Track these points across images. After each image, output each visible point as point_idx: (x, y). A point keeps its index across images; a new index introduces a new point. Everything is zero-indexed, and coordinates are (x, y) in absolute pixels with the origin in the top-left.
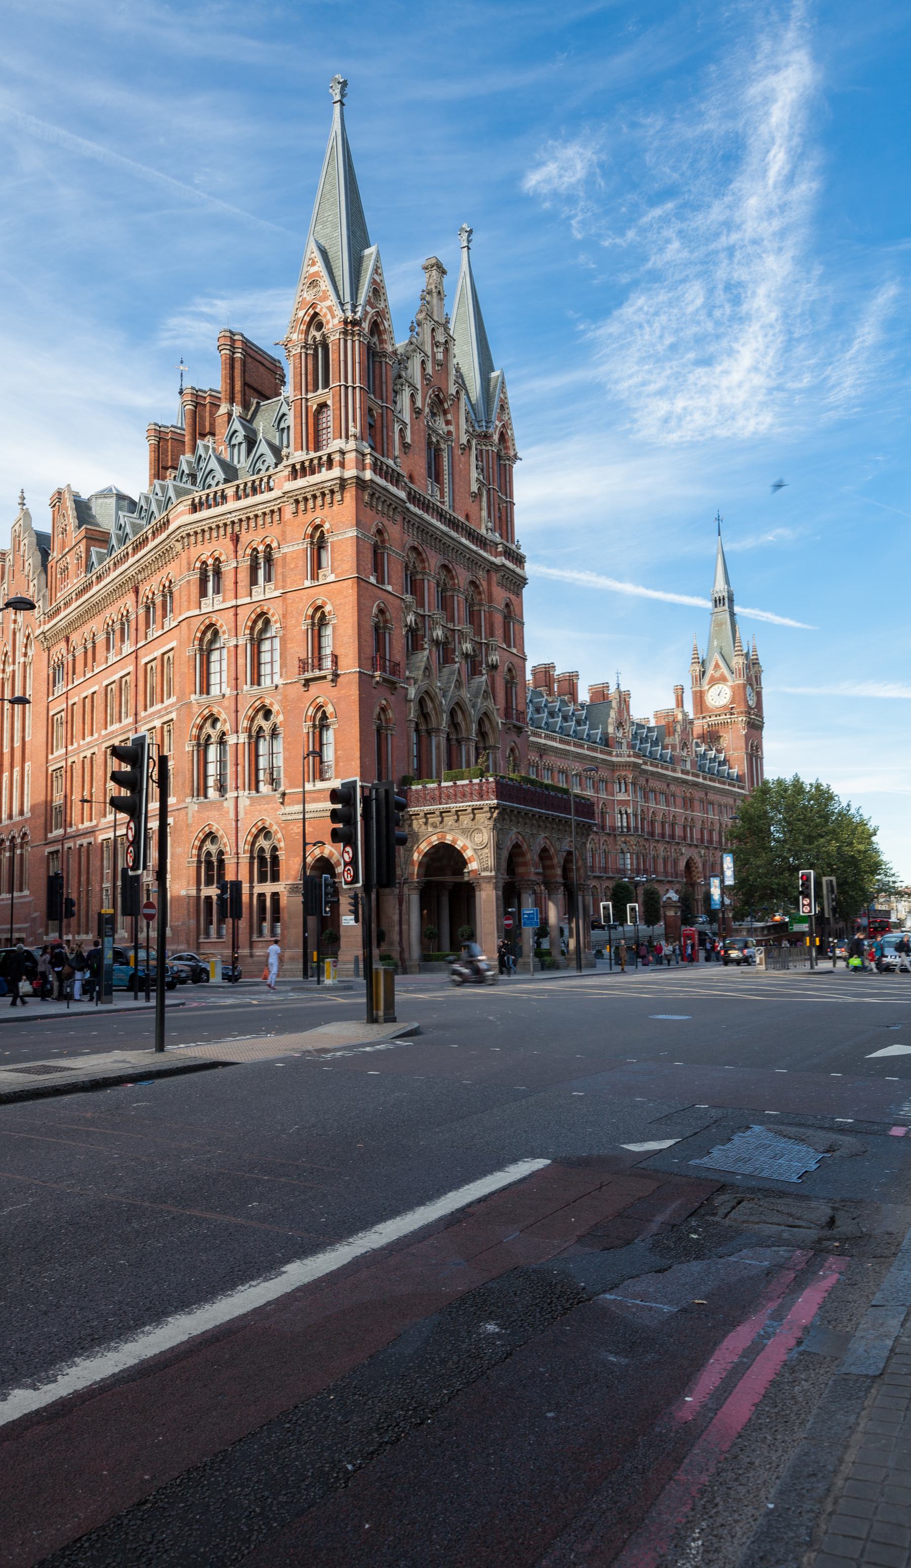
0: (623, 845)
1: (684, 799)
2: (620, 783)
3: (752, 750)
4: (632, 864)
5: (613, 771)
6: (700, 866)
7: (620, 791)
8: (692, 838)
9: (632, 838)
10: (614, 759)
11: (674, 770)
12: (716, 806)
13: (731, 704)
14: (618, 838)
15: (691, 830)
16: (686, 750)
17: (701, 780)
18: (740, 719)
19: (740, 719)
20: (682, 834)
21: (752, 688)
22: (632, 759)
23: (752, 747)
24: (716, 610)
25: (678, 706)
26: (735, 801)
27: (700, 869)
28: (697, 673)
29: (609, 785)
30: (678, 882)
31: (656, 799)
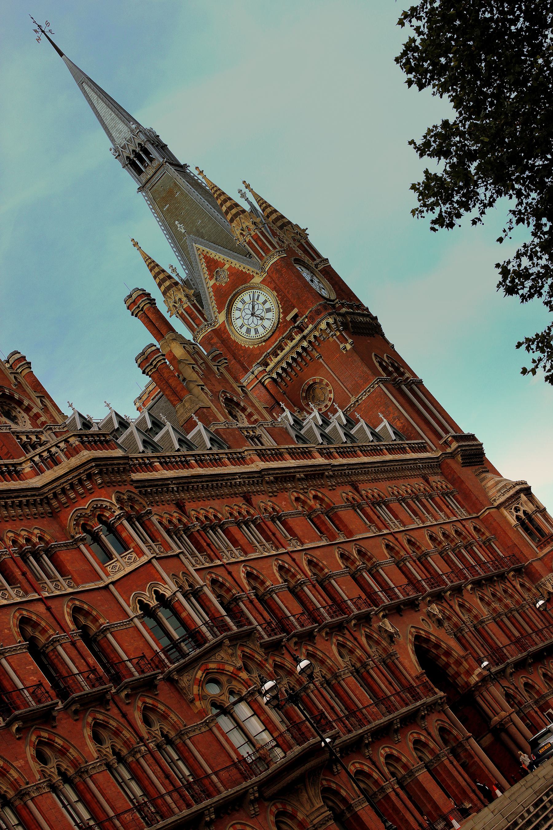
0: (213, 690)
1: (311, 515)
2: (96, 538)
3: (389, 374)
4: (269, 726)
5: (54, 514)
6: (453, 643)
7: (110, 557)
8: (386, 589)
9: (222, 655)
10: (36, 482)
11: (241, 460)
12: (394, 505)
13: (286, 313)
14: (185, 681)
15: (376, 577)
16: (240, 414)
17: (321, 460)
18: (323, 326)
19: (323, 326)
20: (357, 592)
21: (307, 267)
22: (86, 455)
23: (385, 369)
24: (144, 178)
25: (158, 334)
26: (427, 481)
27: (458, 650)
28: (187, 304)
29: (65, 556)
30: (431, 707)
31: (235, 543)
